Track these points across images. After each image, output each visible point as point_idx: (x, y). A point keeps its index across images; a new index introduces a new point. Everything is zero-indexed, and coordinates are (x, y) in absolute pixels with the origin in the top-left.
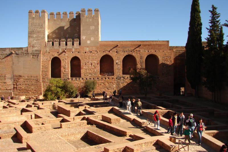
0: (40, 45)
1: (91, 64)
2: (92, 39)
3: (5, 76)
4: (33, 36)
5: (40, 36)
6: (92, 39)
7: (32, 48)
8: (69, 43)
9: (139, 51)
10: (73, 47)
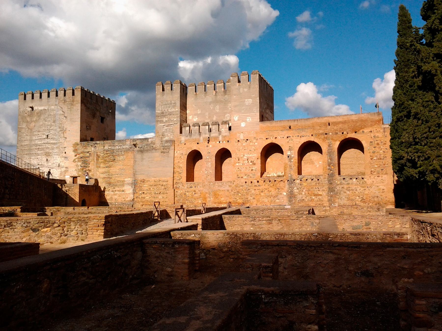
0: (172, 134)
1: (248, 160)
2: (248, 120)
4: (163, 121)
5: (172, 119)
6: (249, 119)
7: (162, 138)
9: (326, 134)
10: (220, 134)
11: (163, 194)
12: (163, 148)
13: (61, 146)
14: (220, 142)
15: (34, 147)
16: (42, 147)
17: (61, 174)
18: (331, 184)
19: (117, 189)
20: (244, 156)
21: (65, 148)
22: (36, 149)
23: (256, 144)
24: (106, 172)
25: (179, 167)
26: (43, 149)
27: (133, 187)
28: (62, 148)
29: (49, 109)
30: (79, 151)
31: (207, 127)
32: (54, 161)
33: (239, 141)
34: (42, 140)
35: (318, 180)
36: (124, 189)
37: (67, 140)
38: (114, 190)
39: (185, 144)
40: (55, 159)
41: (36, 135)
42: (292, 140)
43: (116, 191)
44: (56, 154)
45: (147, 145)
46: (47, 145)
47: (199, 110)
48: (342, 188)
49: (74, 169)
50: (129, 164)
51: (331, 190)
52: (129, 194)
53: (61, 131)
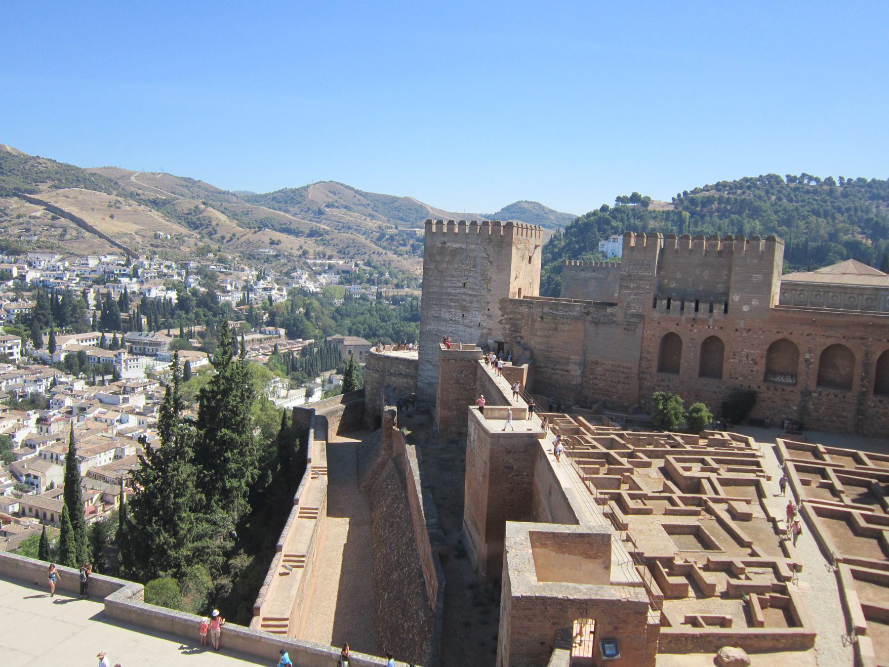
2: (753, 303)
3: (568, 359)
5: (643, 286)
10: (710, 316)
11: (624, 383)
12: (626, 323)
13: (482, 300)
14: (709, 327)
15: (445, 297)
16: (457, 298)
17: (481, 337)
19: (558, 366)
20: (742, 350)
21: (488, 303)
23: (762, 337)
25: (649, 352)
26: (457, 301)
31: (693, 305)
33: (737, 330)
35: (844, 397)
36: (568, 368)
37: (492, 293)
42: (814, 339)
43: (557, 369)
45: (604, 316)
46: (463, 296)
49: (500, 333)
52: (577, 376)
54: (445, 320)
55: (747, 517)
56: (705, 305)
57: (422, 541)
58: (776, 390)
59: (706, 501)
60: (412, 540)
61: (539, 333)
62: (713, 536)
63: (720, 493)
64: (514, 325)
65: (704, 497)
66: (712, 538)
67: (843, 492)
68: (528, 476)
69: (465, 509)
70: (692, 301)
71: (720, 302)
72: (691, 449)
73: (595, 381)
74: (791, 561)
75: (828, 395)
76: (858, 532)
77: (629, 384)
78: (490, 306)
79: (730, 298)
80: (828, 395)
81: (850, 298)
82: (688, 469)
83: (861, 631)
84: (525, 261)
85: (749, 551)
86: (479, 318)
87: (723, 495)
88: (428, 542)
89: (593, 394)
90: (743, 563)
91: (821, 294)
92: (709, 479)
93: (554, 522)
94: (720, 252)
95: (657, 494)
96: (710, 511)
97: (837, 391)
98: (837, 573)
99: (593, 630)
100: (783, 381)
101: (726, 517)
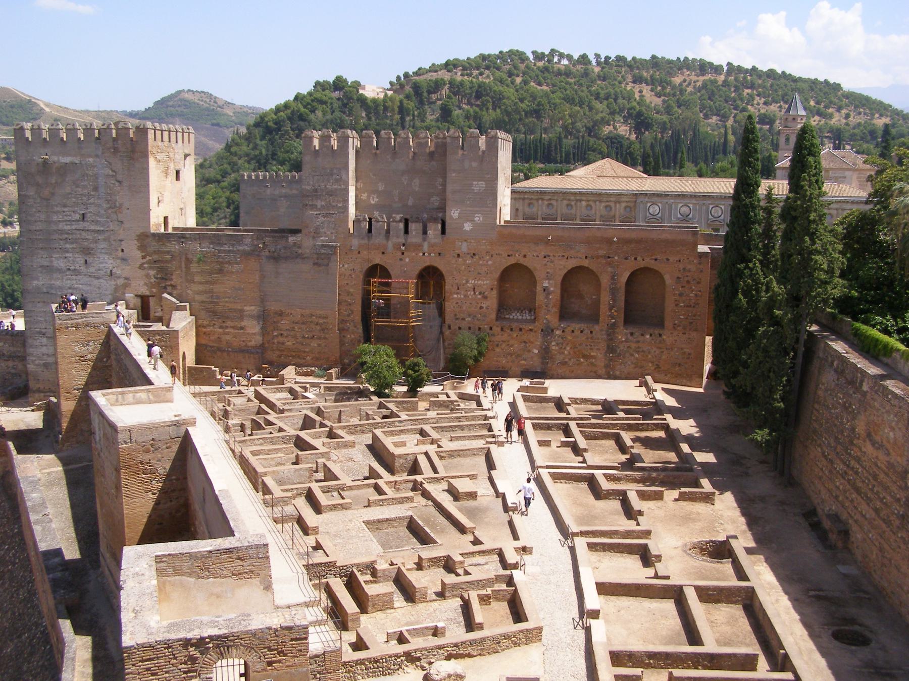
2: (477, 219)
3: (242, 311)
5: (334, 204)
8: (413, 228)
10: (424, 240)
11: (319, 338)
12: (315, 256)
14: (424, 254)
15: (56, 236)
18: (611, 339)
19: (229, 323)
20: (467, 282)
21: (121, 241)
22: (61, 240)
23: (490, 262)
24: (206, 292)
25: (349, 293)
26: (75, 241)
27: (261, 323)
28: (115, 240)
29: (83, 162)
30: (151, 249)
31: (401, 225)
32: (101, 265)
34: (73, 223)
35: (591, 332)
36: (243, 324)
38: (224, 325)
39: (359, 253)
40: (101, 260)
41: (58, 212)
42: (552, 262)
43: (227, 327)
44: (103, 251)
45: (285, 248)
46: (84, 234)
47: (380, 184)
48: (629, 347)
49: (142, 283)
50: (251, 281)
51: (611, 349)
52: (254, 334)
53: (110, 208)
54: (59, 271)
55: (473, 495)
56: (417, 224)
57: (44, 591)
58: (512, 330)
59: (422, 483)
60: (32, 593)
61: (197, 278)
62: (428, 525)
63: (439, 470)
64: (161, 270)
65: (419, 478)
66: (426, 529)
67: (585, 450)
68: (178, 479)
69: (101, 536)
70: (400, 221)
71: (435, 220)
72: (407, 418)
73: (281, 339)
74: (518, 544)
75: (573, 331)
76: (597, 493)
77: (325, 338)
78: (124, 245)
79: (447, 214)
80: (573, 331)
81: (606, 207)
82: (403, 444)
83: (595, 614)
84: (170, 178)
85: (471, 538)
86: (107, 263)
87: (442, 473)
88: (49, 591)
89: (280, 356)
90: (462, 554)
91: (573, 203)
92: (426, 454)
93: (211, 537)
94: (432, 154)
95: (359, 483)
96: (426, 495)
97: (582, 326)
98: (572, 549)
99: (243, 671)
100: (520, 317)
101: (446, 501)
